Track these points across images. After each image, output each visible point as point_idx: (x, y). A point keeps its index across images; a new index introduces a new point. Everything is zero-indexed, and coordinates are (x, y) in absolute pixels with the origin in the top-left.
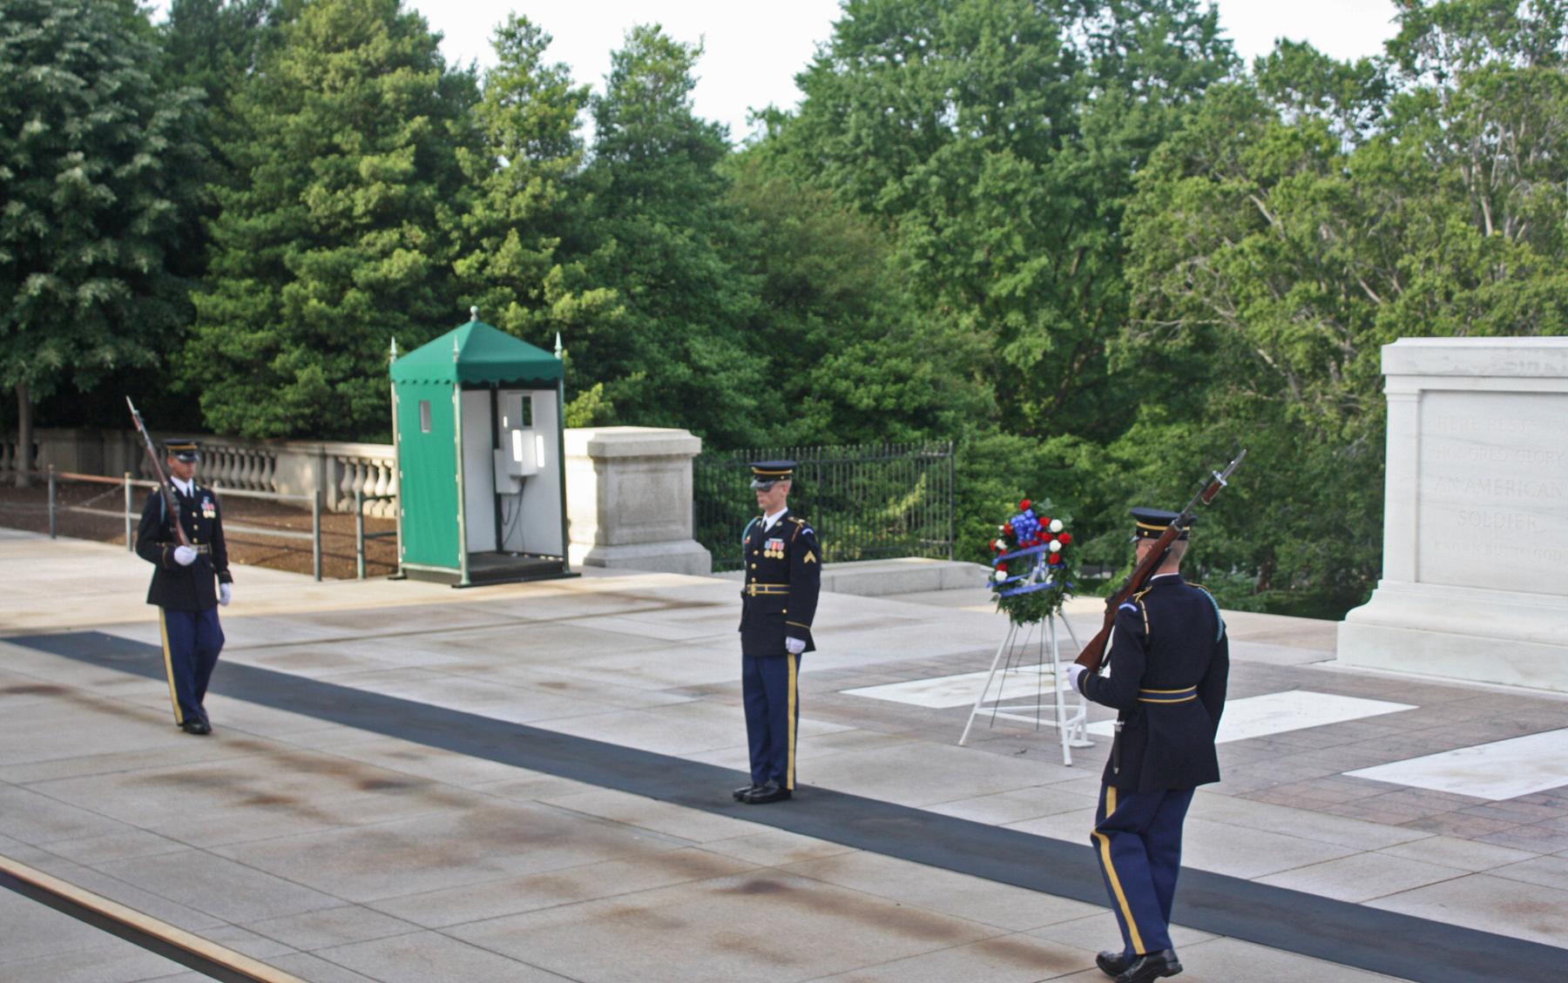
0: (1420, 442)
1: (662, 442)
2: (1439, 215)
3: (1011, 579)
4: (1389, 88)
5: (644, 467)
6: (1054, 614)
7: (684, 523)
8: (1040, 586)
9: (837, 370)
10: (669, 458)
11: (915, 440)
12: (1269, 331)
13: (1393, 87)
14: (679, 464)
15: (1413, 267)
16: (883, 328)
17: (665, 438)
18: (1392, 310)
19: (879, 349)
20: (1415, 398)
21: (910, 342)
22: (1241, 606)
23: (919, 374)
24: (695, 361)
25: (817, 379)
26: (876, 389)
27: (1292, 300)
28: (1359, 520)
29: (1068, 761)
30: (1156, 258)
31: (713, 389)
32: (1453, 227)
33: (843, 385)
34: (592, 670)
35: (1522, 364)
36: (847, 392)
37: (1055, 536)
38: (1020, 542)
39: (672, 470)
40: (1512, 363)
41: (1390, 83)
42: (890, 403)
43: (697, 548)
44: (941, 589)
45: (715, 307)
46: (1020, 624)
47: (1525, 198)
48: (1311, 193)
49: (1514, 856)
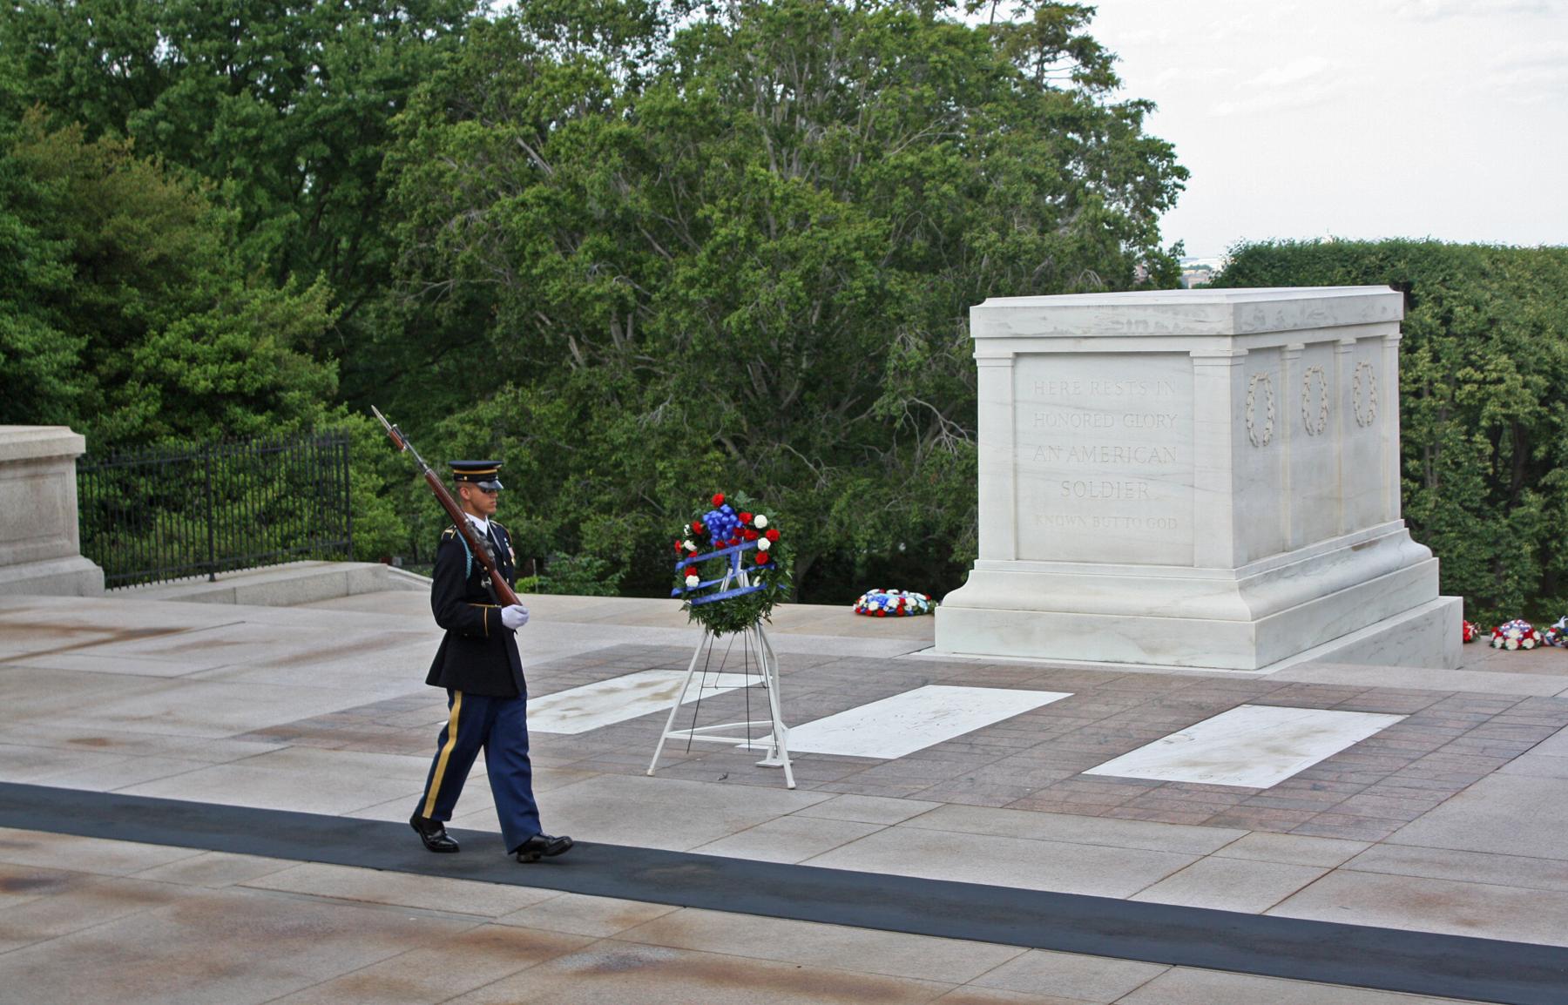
0: (1015, 408)
1: (42, 442)
2: (738, 161)
3: (704, 584)
4: (659, 23)
5: (22, 472)
6: (762, 620)
7: (70, 538)
8: (737, 593)
9: (166, 349)
10: (49, 460)
11: (258, 427)
12: (563, 290)
13: (665, 23)
14: (61, 467)
15: (714, 217)
16: (210, 299)
17: (25, 438)
18: (694, 265)
19: (209, 322)
20: (1009, 363)
21: (245, 314)
22: (592, 591)
23: (260, 350)
24: (7, 345)
25: (140, 361)
26: (213, 369)
27: (582, 254)
28: (668, 491)
29: (791, 784)
30: (426, 211)
31: (30, 375)
32: (753, 173)
33: (172, 366)
34: (114, 719)
35: (1129, 323)
36: (179, 374)
37: (762, 532)
38: (713, 541)
39: (54, 475)
40: (1118, 323)
41: (661, 18)
42: (229, 385)
43: (87, 564)
44: (348, 595)
45: (21, 279)
46: (717, 634)
47: (820, 141)
48: (600, 137)
49: (1353, 847)
